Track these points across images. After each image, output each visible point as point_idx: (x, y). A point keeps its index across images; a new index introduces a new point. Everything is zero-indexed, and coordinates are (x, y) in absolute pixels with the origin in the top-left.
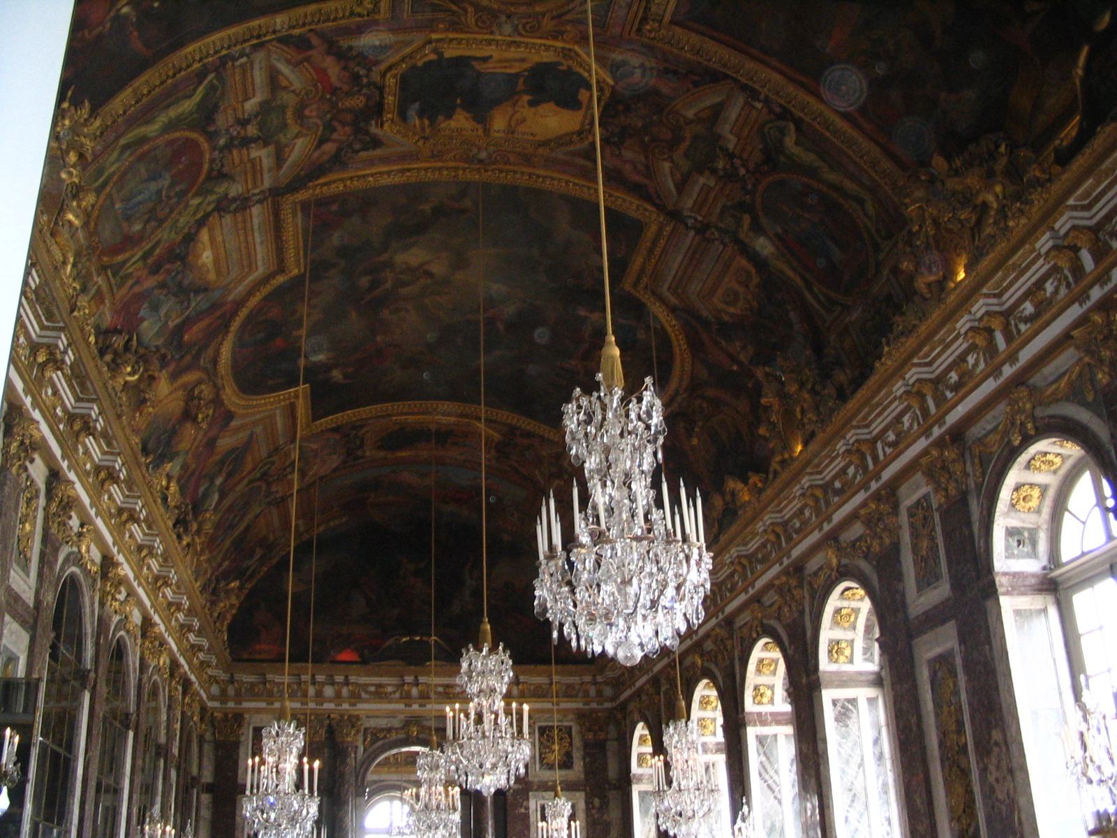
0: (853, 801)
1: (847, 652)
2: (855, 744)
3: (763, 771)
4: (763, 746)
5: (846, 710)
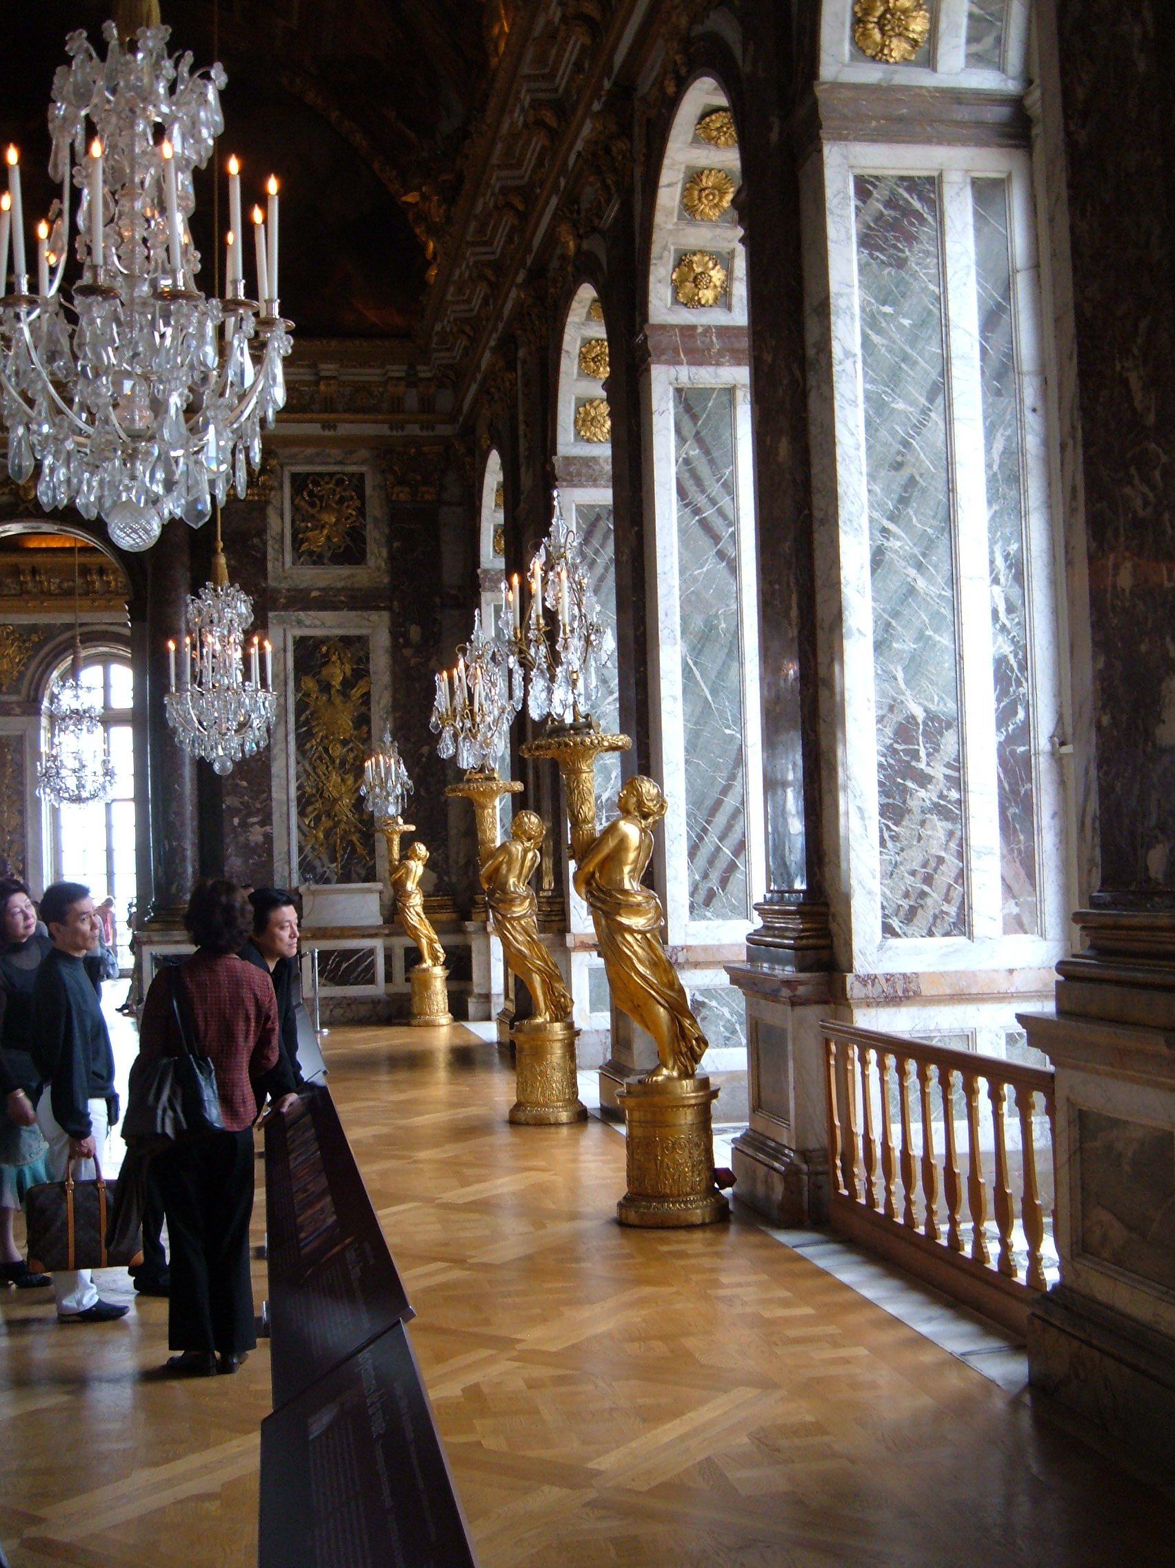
0: (903, 501)
1: (918, 25)
2: (922, 324)
3: (690, 485)
4: (694, 418)
5: (900, 218)
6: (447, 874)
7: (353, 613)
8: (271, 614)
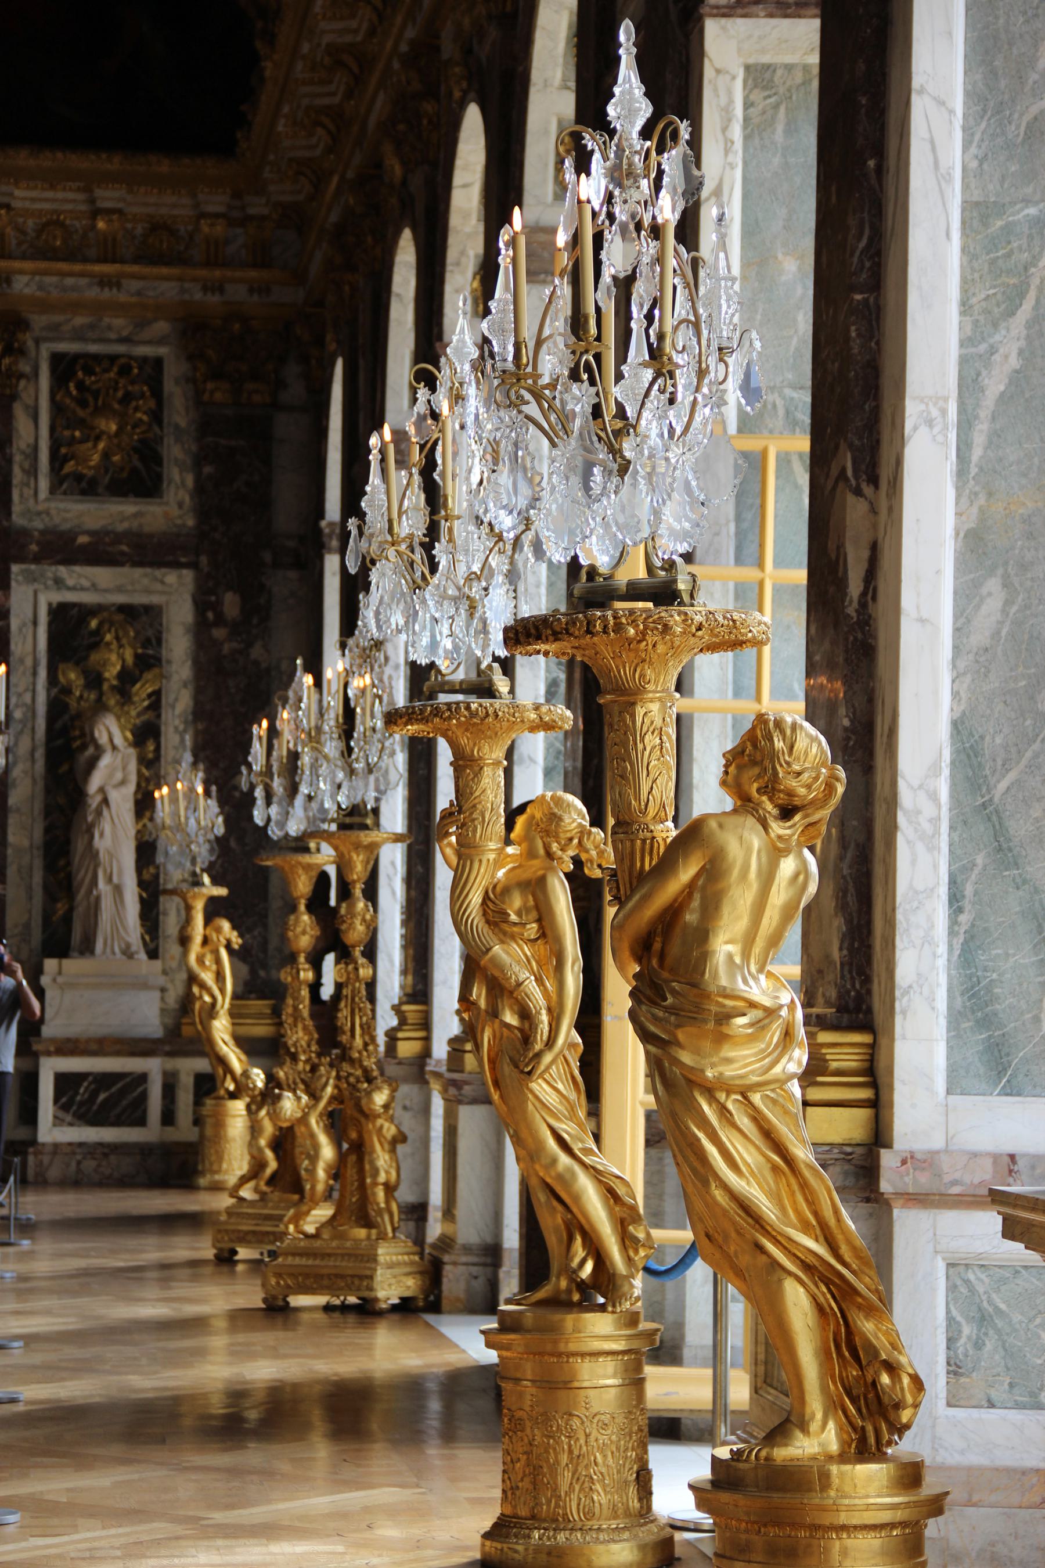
6: (265, 966)
7: (138, 572)
8: (15, 568)
